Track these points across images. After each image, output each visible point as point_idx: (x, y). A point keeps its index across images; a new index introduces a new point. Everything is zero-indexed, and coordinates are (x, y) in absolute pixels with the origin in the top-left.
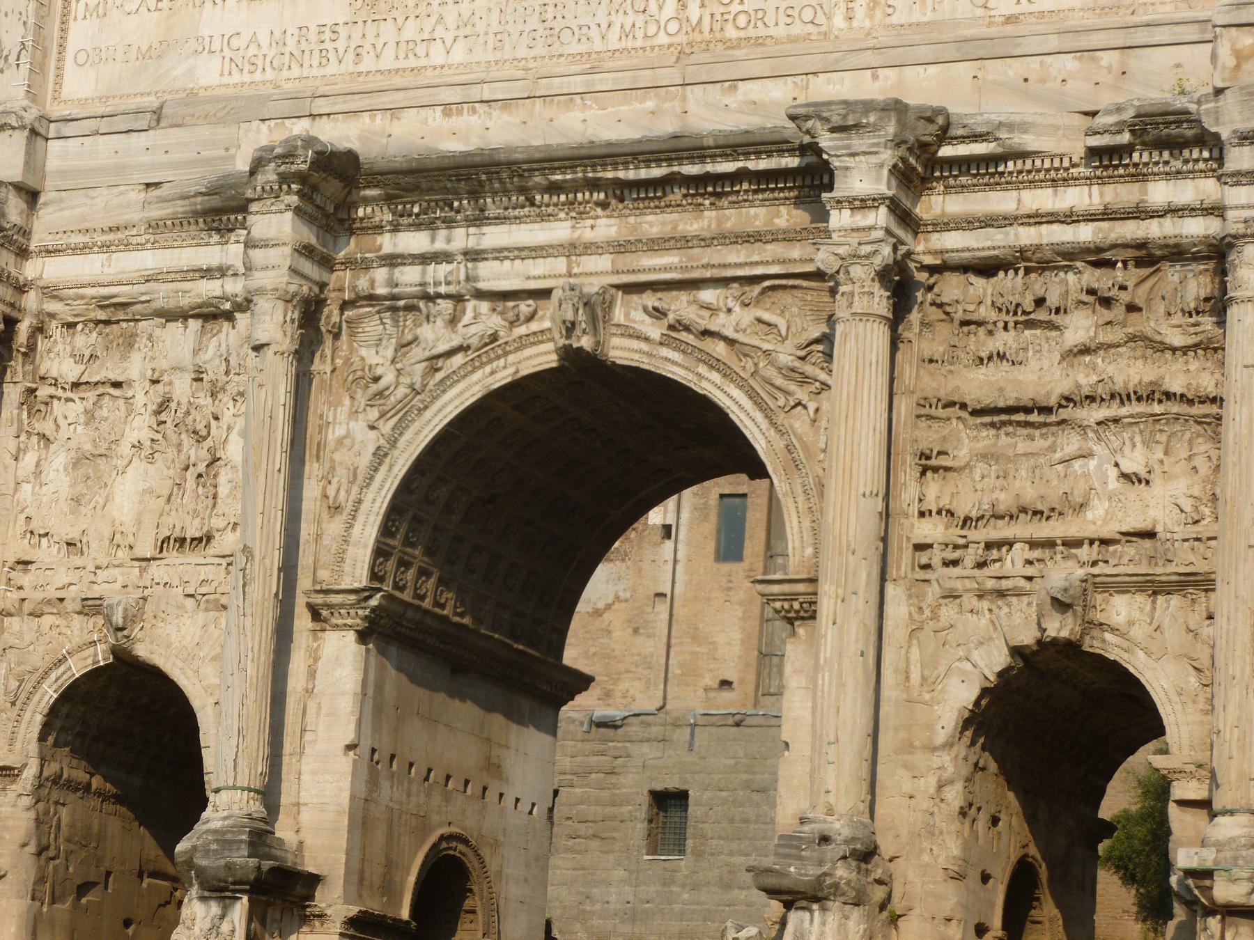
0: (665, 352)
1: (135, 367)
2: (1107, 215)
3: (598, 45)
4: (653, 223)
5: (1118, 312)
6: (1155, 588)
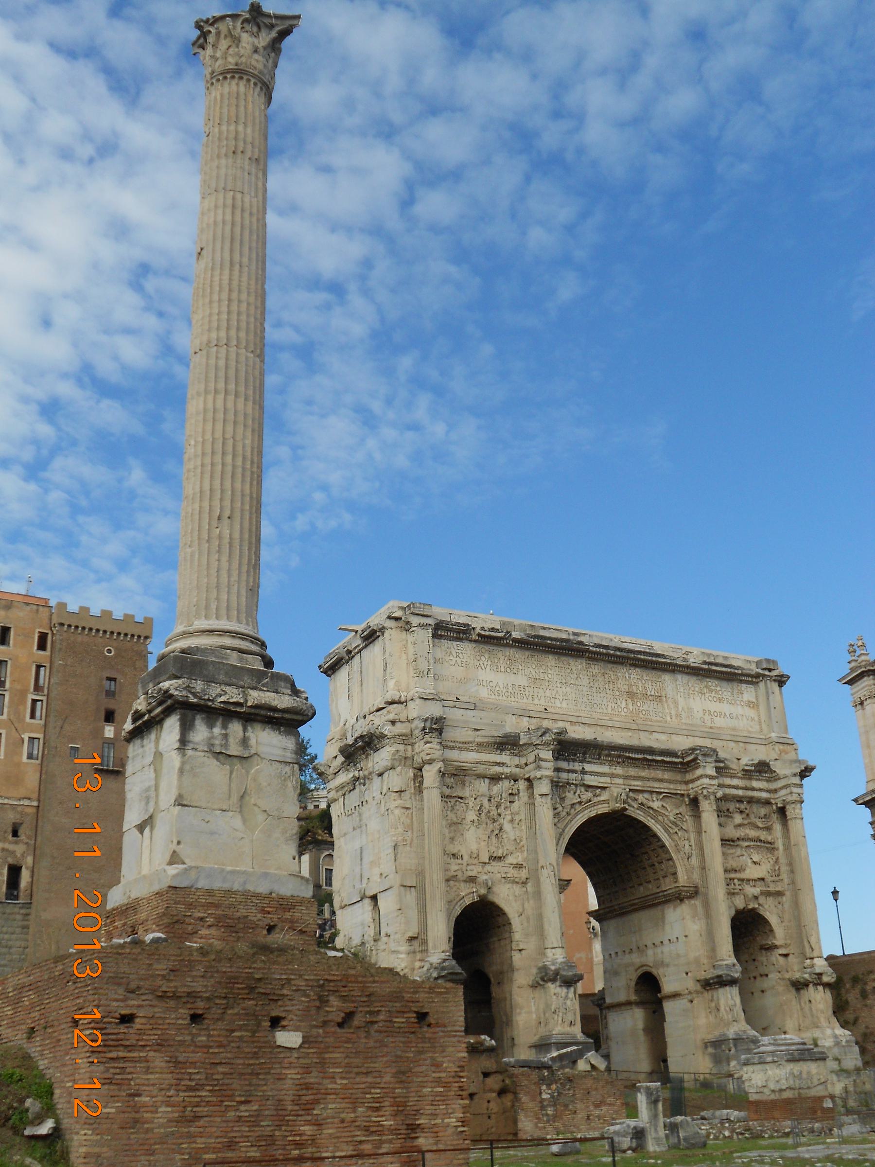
0: (638, 812)
1: (466, 792)
2: (746, 789)
3: (605, 711)
4: (632, 772)
5: (744, 816)
6: (768, 894)
